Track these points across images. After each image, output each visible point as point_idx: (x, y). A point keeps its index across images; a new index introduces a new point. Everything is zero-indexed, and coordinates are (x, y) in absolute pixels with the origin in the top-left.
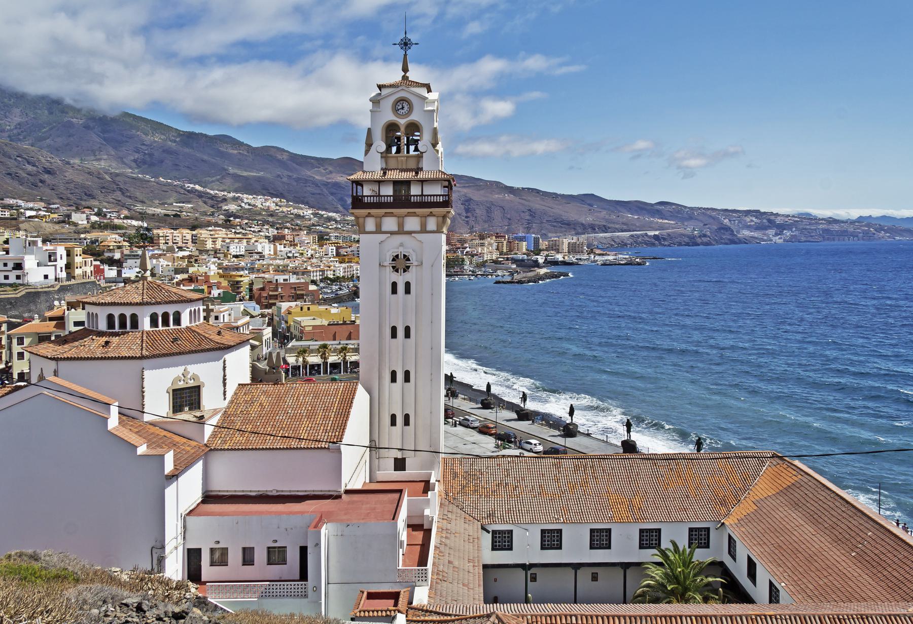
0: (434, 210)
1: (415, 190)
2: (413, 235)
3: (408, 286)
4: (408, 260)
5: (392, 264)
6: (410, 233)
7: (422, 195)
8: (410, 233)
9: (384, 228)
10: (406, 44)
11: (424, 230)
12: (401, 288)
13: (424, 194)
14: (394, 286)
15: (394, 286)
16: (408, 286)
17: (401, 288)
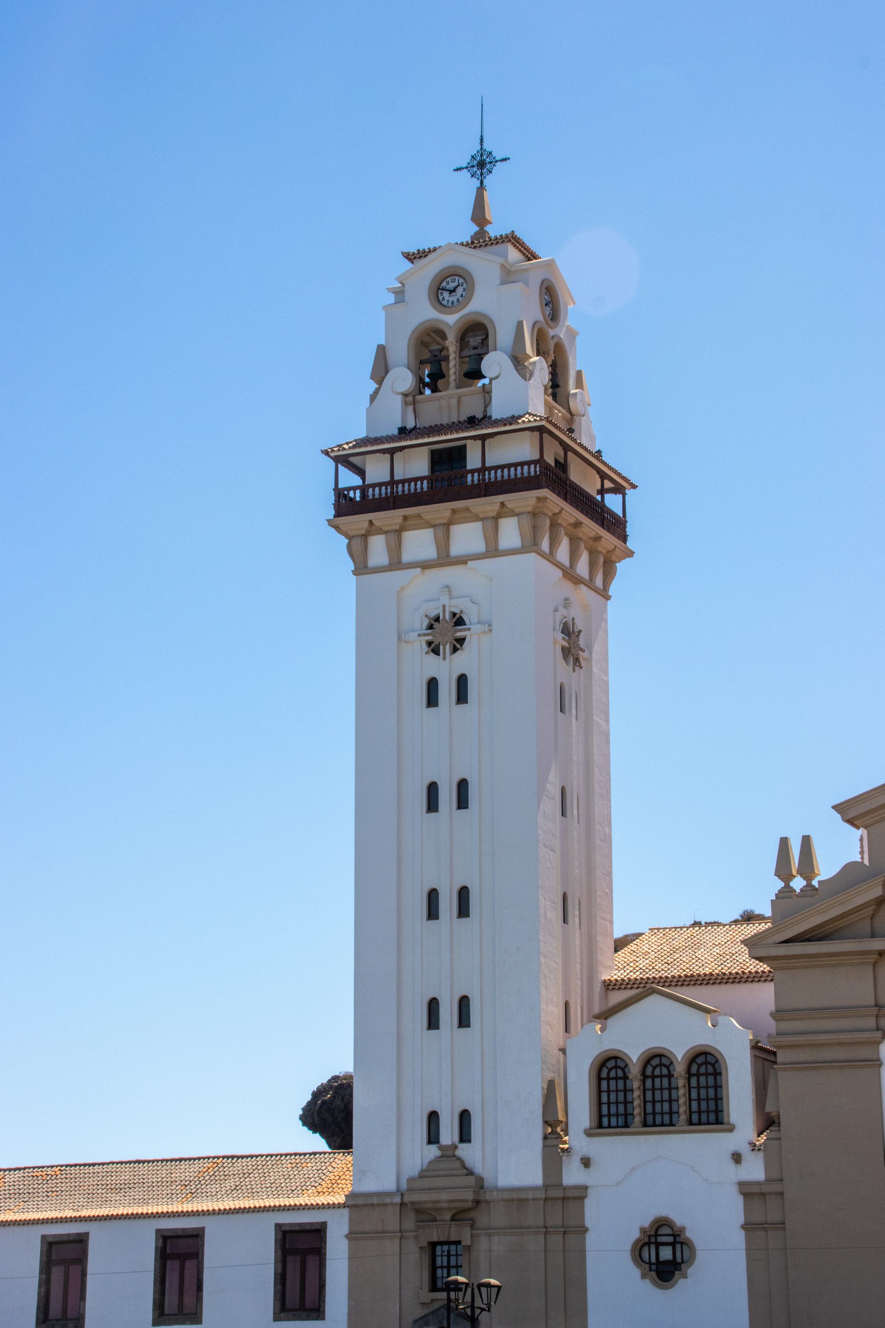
0: (514, 500)
1: (473, 461)
2: (470, 564)
3: (462, 681)
4: (459, 621)
5: (425, 635)
6: (462, 561)
7: (483, 469)
8: (462, 561)
9: (407, 557)
10: (481, 165)
11: (493, 551)
12: (447, 691)
13: (487, 465)
14: (432, 685)
15: (432, 685)
16: (462, 681)
17: (447, 691)
